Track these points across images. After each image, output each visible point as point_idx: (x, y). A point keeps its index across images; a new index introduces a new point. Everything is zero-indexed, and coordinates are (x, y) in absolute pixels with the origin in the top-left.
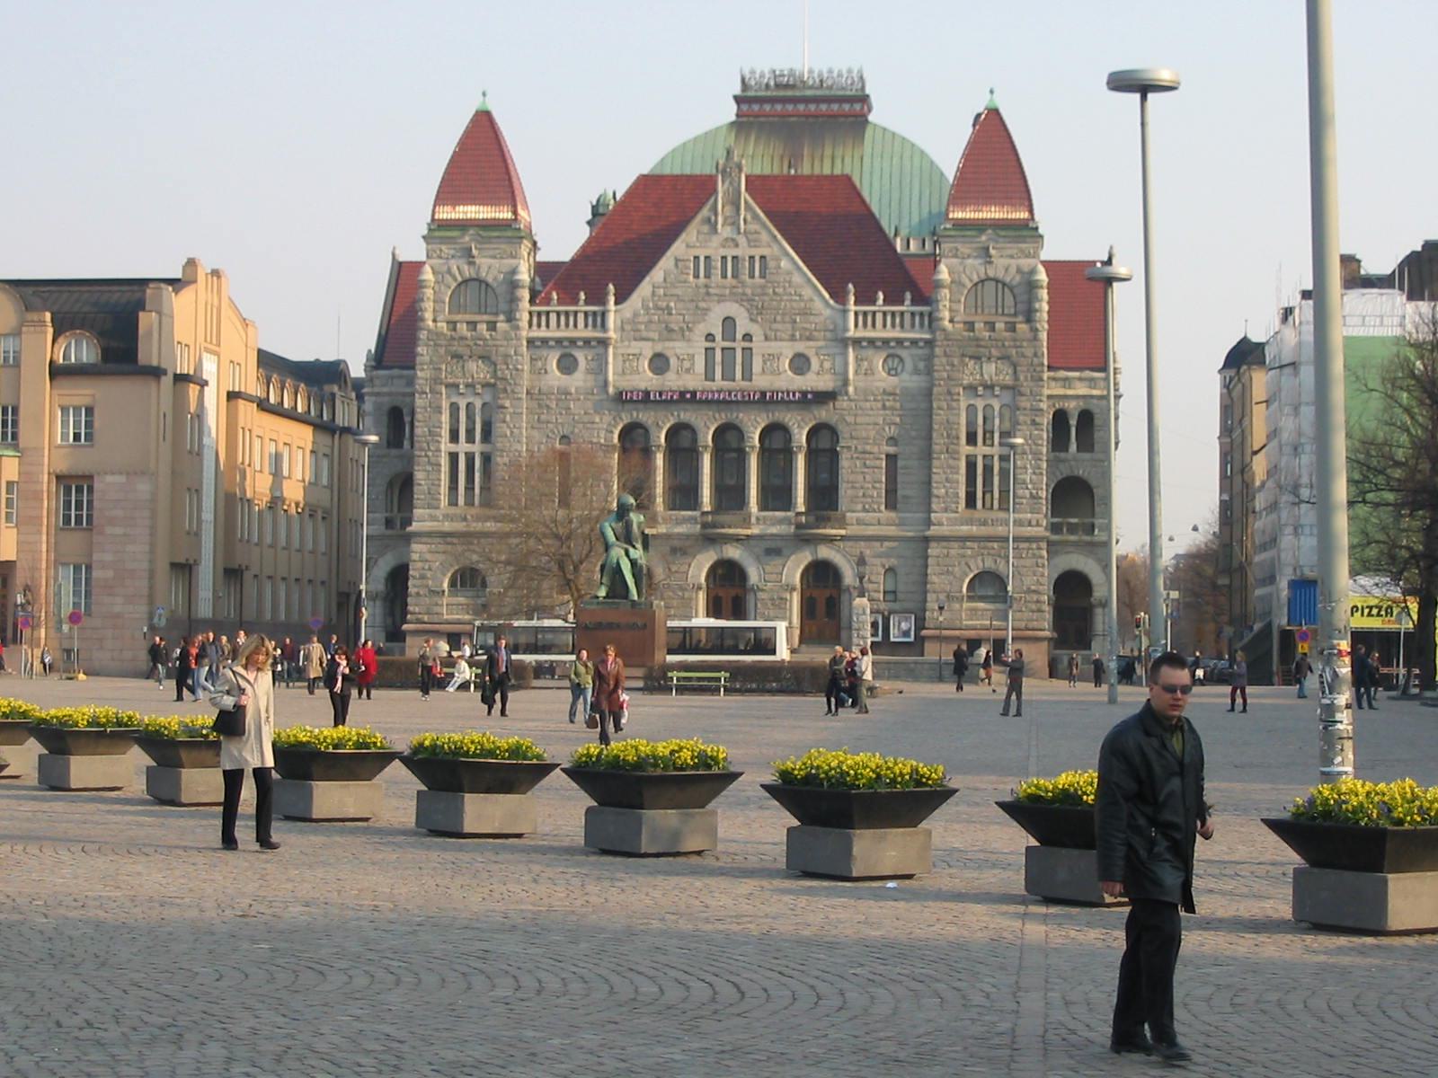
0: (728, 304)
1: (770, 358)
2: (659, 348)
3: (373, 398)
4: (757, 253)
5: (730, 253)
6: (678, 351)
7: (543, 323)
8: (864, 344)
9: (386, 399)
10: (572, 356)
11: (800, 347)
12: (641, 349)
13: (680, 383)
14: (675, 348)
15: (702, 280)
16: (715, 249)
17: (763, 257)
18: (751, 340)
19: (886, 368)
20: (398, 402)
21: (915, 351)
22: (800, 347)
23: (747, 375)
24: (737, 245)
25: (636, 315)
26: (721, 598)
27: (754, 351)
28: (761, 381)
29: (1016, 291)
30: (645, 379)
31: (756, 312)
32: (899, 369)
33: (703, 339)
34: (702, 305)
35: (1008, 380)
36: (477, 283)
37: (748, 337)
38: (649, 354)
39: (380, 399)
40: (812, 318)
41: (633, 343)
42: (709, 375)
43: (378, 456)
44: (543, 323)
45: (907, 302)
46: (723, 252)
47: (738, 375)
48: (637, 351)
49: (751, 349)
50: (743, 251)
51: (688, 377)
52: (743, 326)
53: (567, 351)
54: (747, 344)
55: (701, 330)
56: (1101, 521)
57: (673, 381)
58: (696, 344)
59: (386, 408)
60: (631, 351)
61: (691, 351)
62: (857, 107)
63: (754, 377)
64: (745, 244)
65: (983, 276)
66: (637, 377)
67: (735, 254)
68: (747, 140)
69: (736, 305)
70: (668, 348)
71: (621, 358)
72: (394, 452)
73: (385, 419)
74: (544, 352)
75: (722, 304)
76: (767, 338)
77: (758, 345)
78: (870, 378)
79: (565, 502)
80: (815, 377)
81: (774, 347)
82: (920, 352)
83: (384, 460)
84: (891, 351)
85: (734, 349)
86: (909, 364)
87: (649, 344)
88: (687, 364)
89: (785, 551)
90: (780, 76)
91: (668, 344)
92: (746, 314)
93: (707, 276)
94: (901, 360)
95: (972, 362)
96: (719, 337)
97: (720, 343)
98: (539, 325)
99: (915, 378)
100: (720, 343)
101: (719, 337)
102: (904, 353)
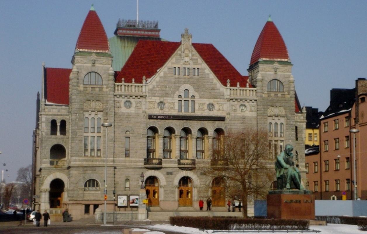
0: (186, 85)
1: (200, 104)
2: (162, 100)
3: (45, 116)
4: (196, 67)
5: (187, 67)
6: (169, 101)
7: (120, 89)
8: (234, 100)
9: (50, 117)
10: (129, 102)
11: (211, 101)
12: (155, 99)
13: (170, 113)
14: (168, 100)
15: (177, 76)
16: (181, 65)
17: (198, 69)
18: (194, 98)
19: (240, 109)
20: (55, 118)
21: (251, 103)
22: (211, 101)
23: (193, 111)
24: (189, 64)
25: (154, 87)
26: (183, 190)
27: (196, 102)
28: (198, 113)
29: (284, 84)
30: (157, 111)
31: (197, 89)
32: (245, 110)
33: (178, 97)
34: (177, 85)
35: (283, 113)
36: (94, 74)
37: (193, 96)
38: (158, 101)
39: (48, 117)
40: (216, 91)
41: (153, 98)
42: (180, 111)
43: (47, 138)
44: (120, 89)
45: (238, 86)
46: (184, 66)
47: (190, 110)
48: (154, 101)
49: (194, 101)
50: (192, 66)
51: (172, 110)
52: (192, 92)
53: (129, 99)
54: (193, 100)
55: (177, 93)
56: (301, 164)
57: (167, 112)
58: (175, 99)
59: (50, 120)
60: (152, 101)
61: (173, 101)
62: (157, 33)
63: (196, 111)
64: (192, 64)
65: (273, 78)
66: (154, 110)
67: (189, 67)
68: (124, 41)
69: (189, 85)
70: (165, 100)
71: (148, 103)
72: (53, 136)
73: (50, 124)
74: (121, 99)
75: (184, 85)
76: (200, 98)
77: (197, 100)
78: (236, 112)
79: (127, 155)
80: (217, 112)
81: (203, 100)
82: (253, 104)
83: (50, 139)
84: (242, 103)
85: (188, 101)
86: (248, 108)
87: (158, 98)
88: (172, 106)
89: (174, 173)
90: (132, 22)
91: (165, 98)
92: (193, 89)
93: (179, 75)
94: (245, 106)
95: (271, 107)
96: (183, 97)
97: (183, 99)
98: (118, 90)
99: (251, 113)
100: (183, 99)
101: (183, 97)
102: (246, 104)
